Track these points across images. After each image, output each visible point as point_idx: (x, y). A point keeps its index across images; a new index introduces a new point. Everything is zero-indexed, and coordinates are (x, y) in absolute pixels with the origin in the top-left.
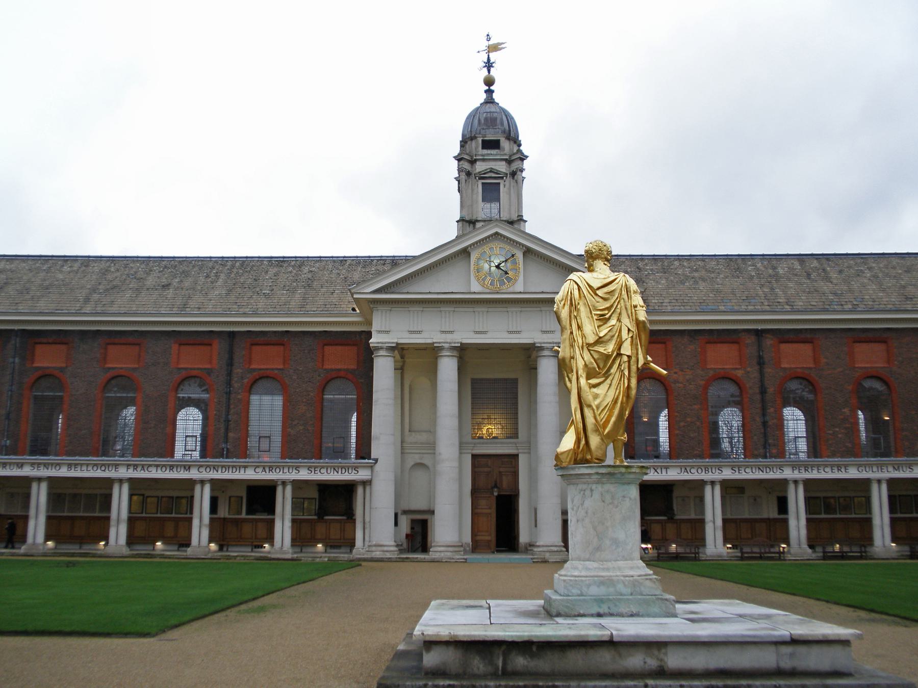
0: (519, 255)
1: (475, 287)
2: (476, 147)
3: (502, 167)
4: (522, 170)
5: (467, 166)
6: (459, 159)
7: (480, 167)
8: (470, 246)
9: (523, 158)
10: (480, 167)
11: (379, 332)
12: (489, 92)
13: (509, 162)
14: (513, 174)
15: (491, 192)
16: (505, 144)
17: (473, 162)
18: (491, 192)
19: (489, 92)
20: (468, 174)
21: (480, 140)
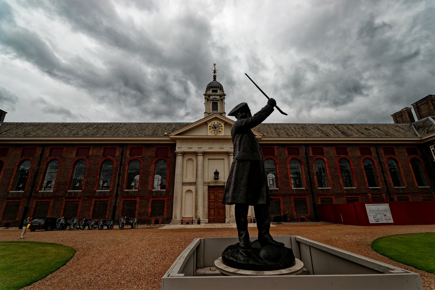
0: (223, 124)
1: (209, 134)
2: (210, 92)
3: (218, 97)
4: (224, 98)
5: (207, 97)
6: (205, 95)
7: (212, 97)
8: (207, 121)
9: (225, 95)
10: (212, 97)
11: (178, 148)
12: (215, 77)
13: (220, 96)
14: (222, 100)
15: (215, 106)
16: (218, 91)
17: (209, 96)
18: (215, 106)
19: (215, 77)
20: (208, 100)
21: (211, 90)
